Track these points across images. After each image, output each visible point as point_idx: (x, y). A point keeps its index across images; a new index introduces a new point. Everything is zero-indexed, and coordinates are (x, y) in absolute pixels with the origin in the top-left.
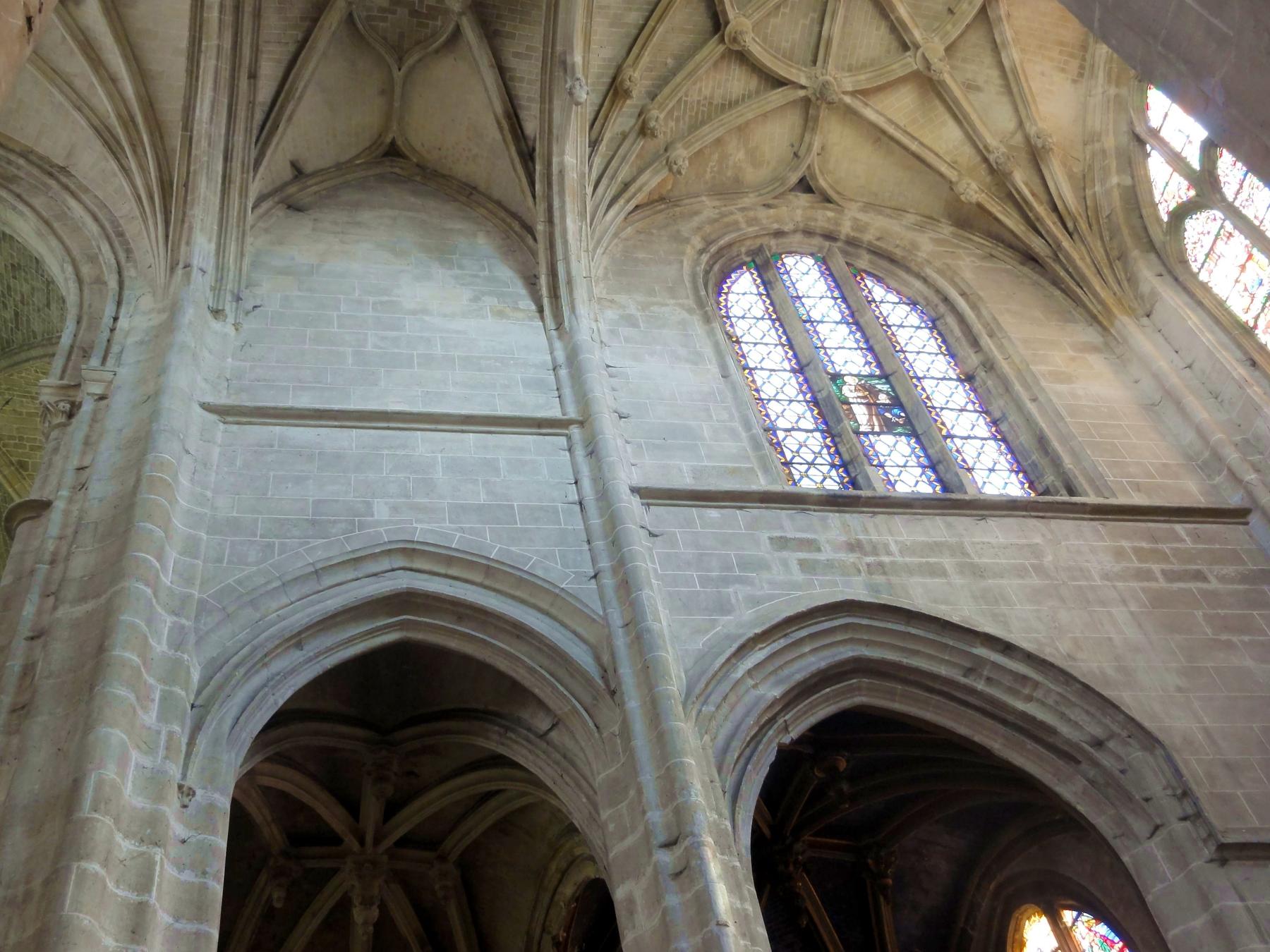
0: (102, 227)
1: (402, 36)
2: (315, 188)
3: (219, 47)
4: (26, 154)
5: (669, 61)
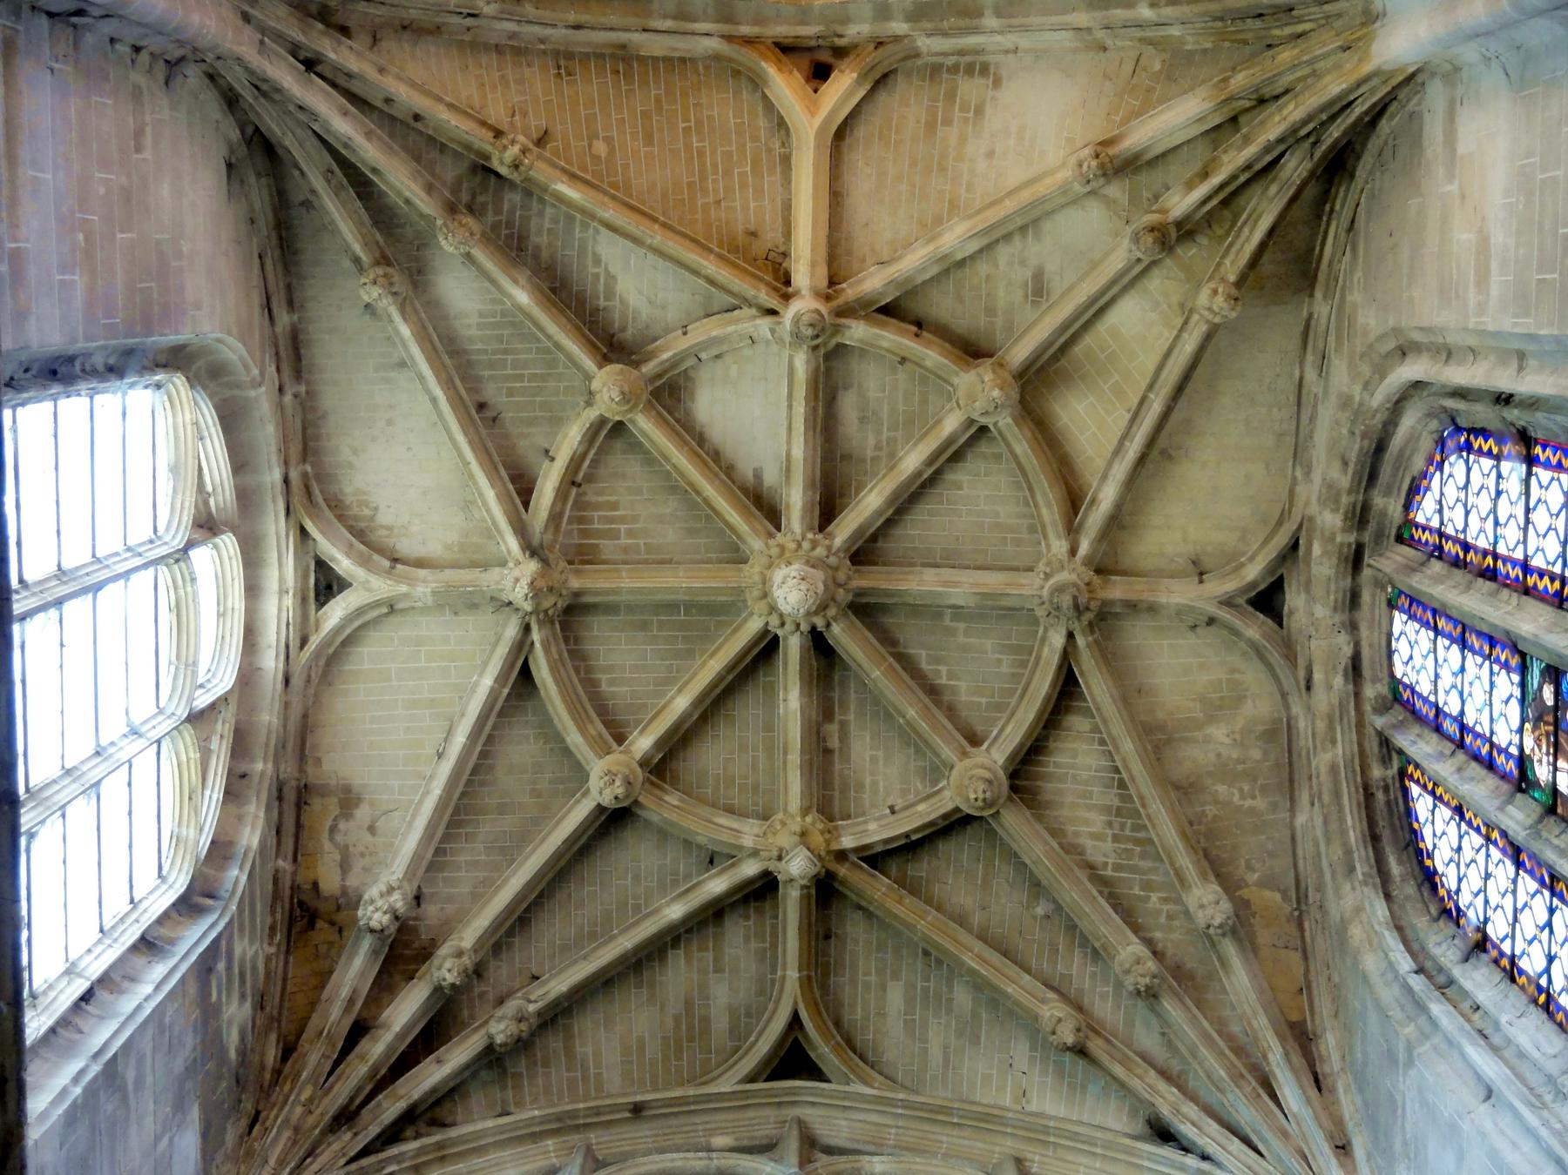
5: (1040, 911)
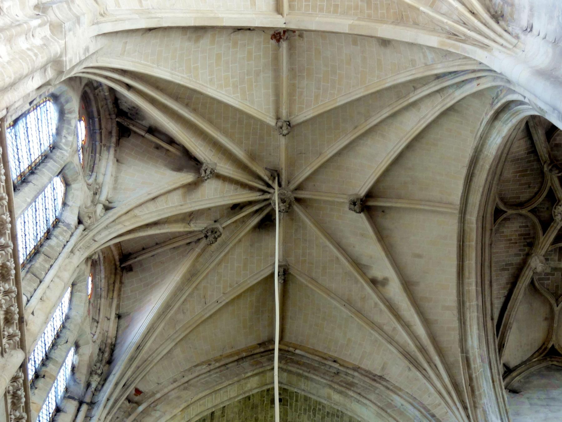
0: (421, 412)
1: (557, 287)
2: (518, 378)
3: (477, 305)
4: (356, 369)
